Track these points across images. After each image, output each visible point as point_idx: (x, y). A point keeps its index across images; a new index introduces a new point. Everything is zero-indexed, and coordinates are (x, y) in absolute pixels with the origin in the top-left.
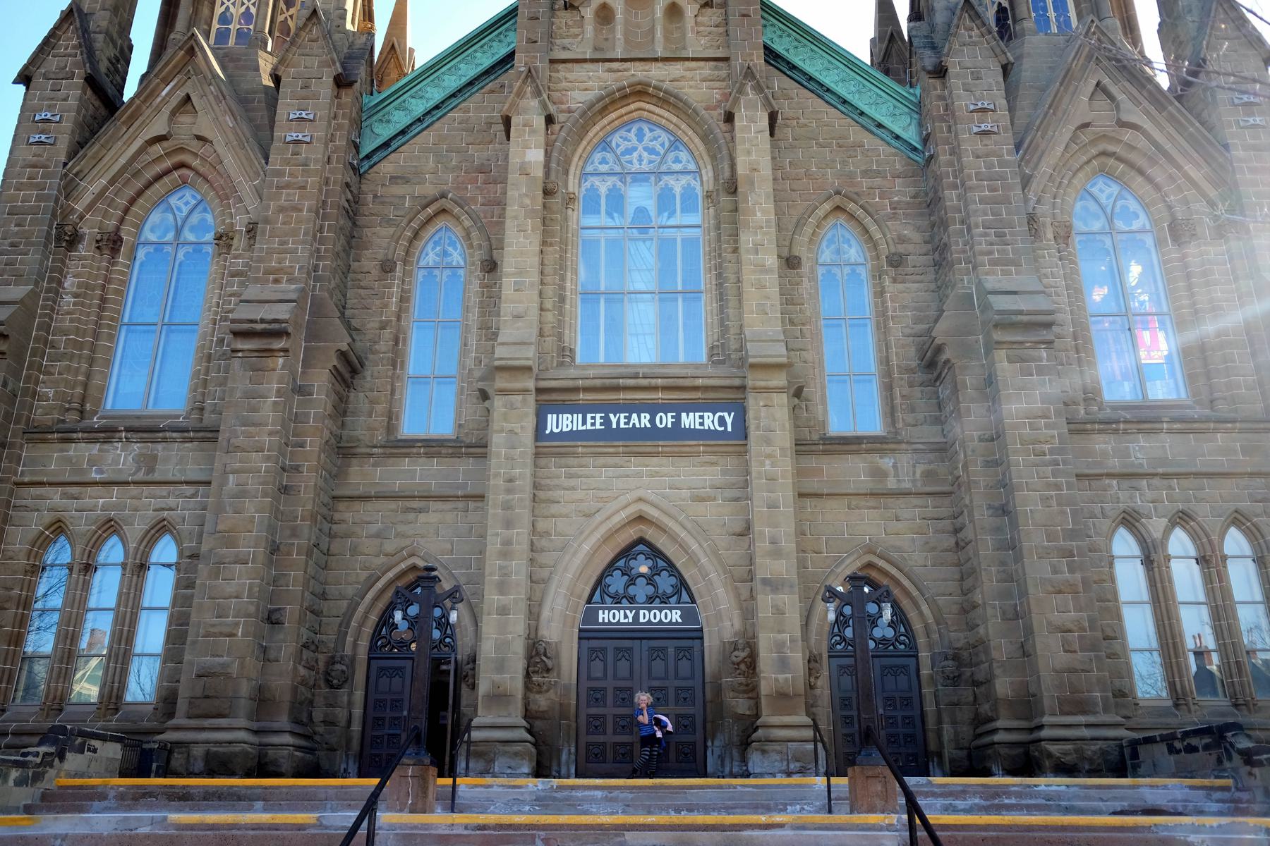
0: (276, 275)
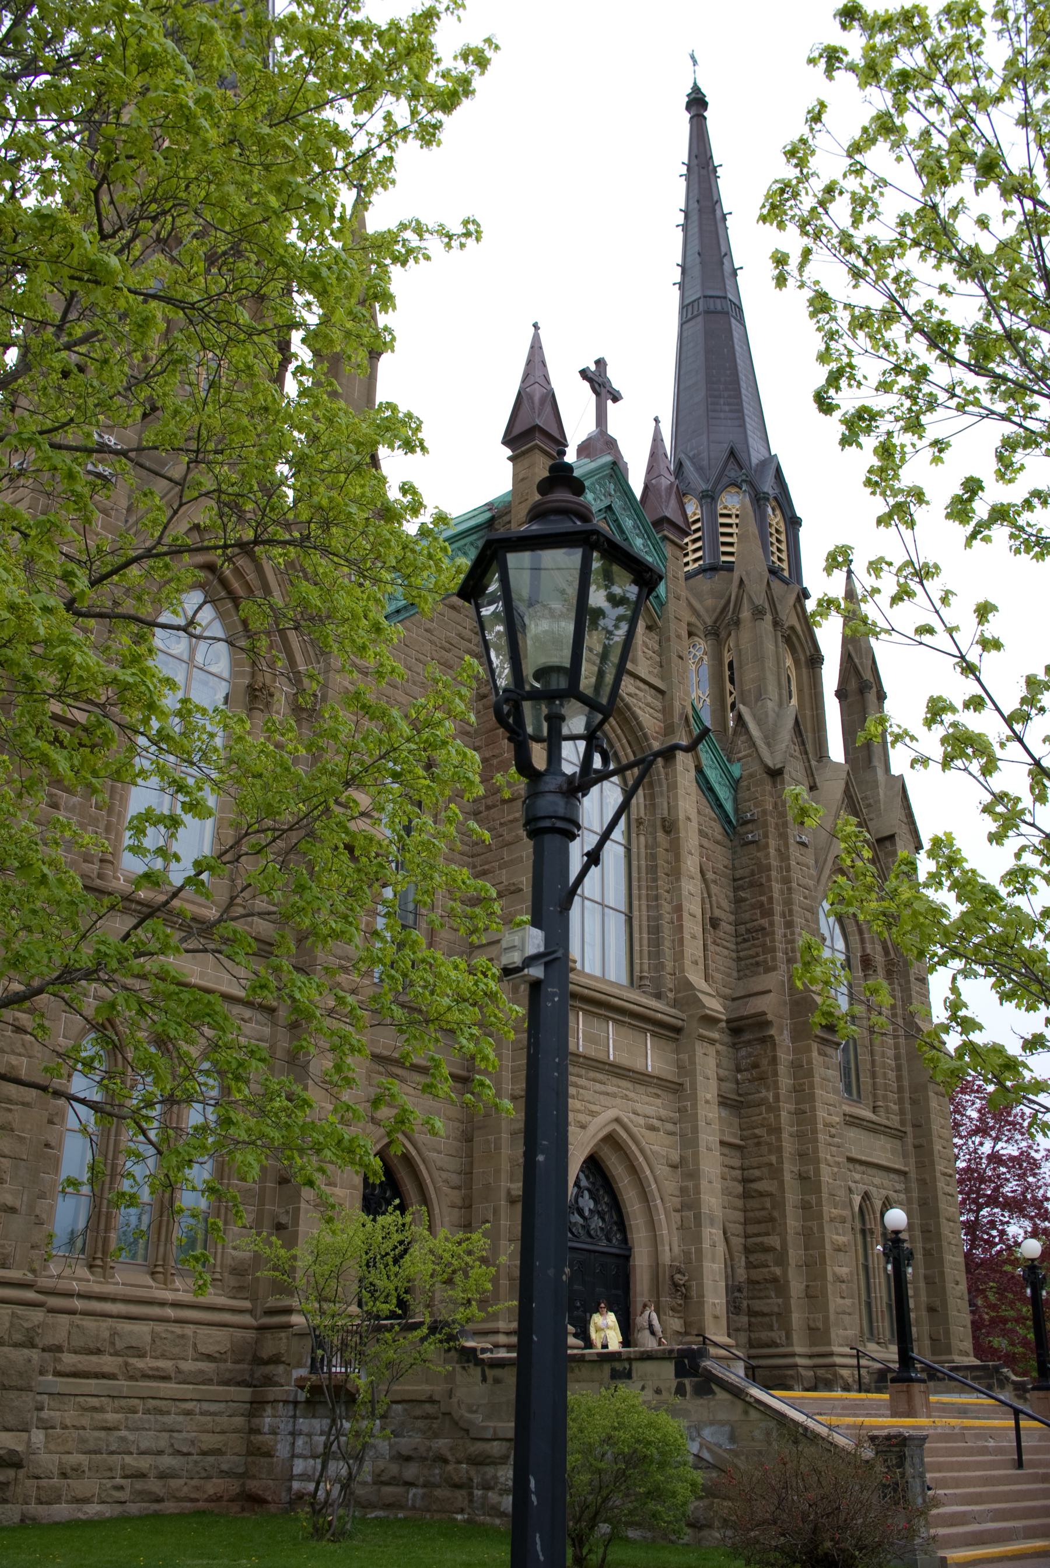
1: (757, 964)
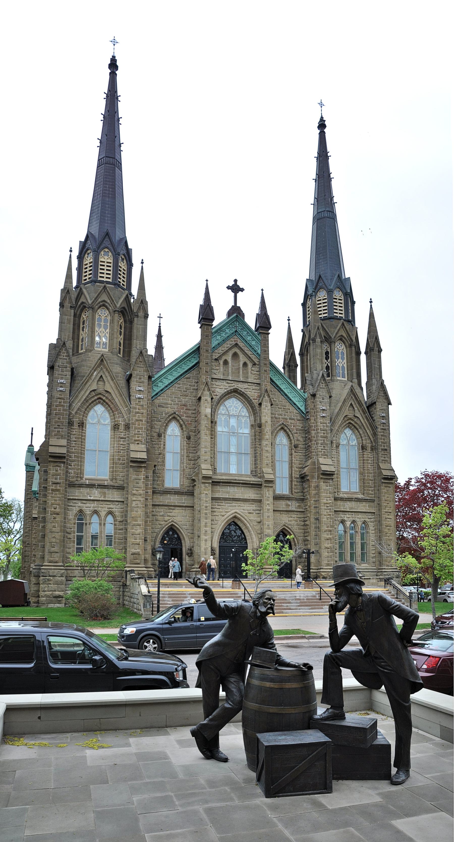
0: (138, 442)
1: (309, 457)
